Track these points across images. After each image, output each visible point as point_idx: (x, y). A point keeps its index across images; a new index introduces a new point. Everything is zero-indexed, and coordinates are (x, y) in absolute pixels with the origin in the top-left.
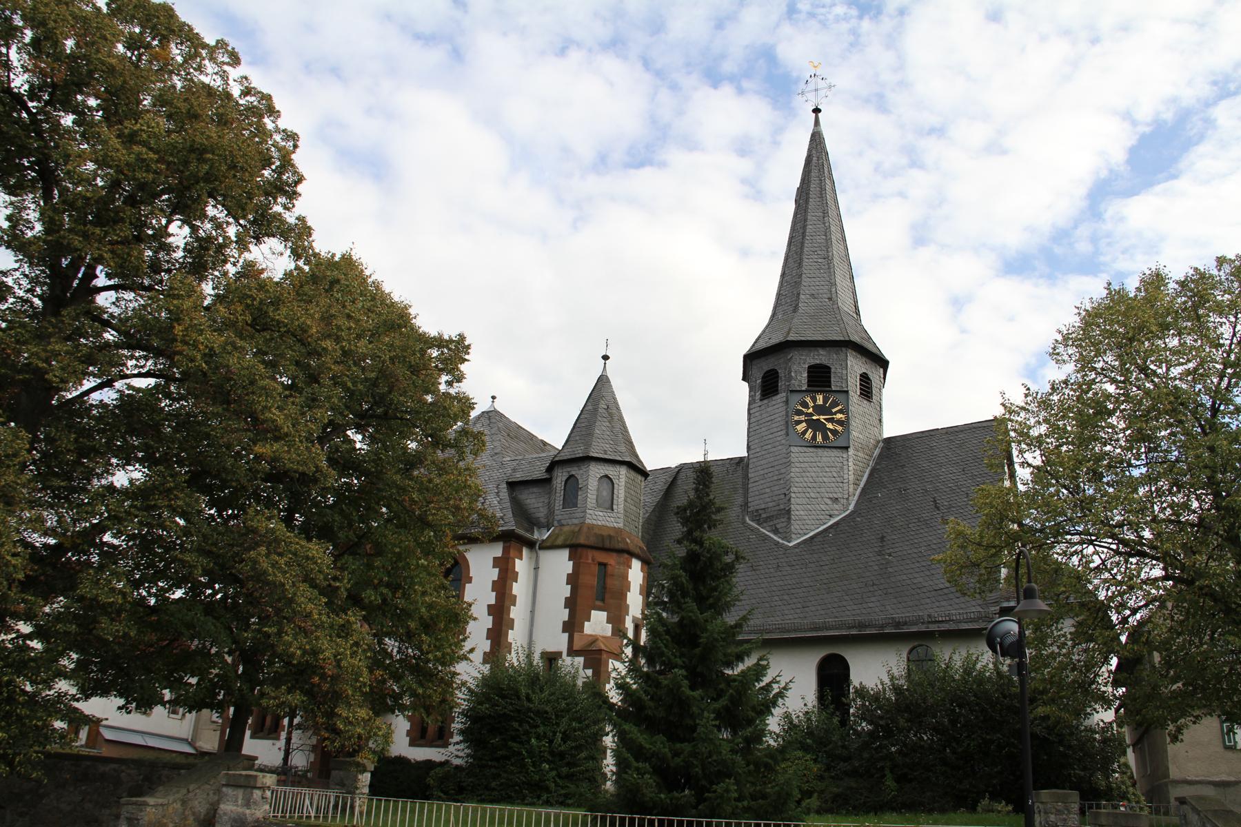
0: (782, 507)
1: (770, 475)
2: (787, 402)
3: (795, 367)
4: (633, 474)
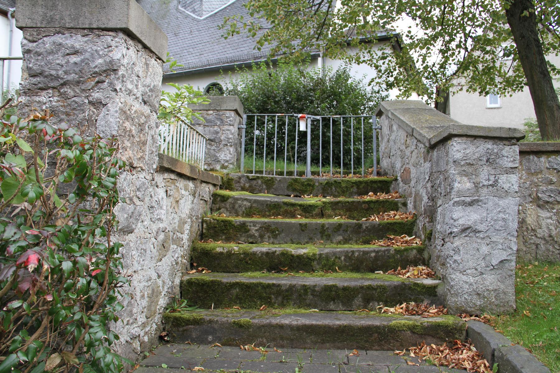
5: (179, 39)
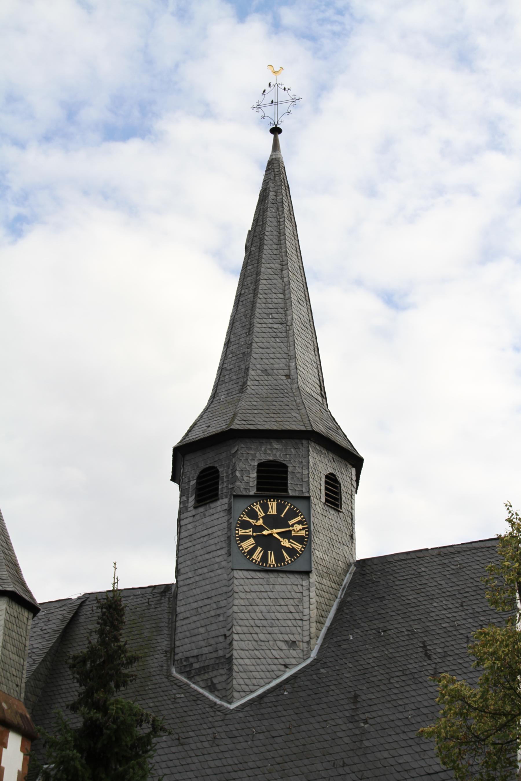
0: (221, 653)
1: (205, 609)
2: (229, 511)
3: (240, 465)
4: (16, 609)
5: (192, 754)
